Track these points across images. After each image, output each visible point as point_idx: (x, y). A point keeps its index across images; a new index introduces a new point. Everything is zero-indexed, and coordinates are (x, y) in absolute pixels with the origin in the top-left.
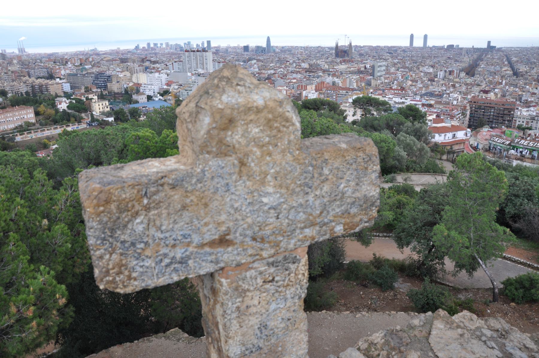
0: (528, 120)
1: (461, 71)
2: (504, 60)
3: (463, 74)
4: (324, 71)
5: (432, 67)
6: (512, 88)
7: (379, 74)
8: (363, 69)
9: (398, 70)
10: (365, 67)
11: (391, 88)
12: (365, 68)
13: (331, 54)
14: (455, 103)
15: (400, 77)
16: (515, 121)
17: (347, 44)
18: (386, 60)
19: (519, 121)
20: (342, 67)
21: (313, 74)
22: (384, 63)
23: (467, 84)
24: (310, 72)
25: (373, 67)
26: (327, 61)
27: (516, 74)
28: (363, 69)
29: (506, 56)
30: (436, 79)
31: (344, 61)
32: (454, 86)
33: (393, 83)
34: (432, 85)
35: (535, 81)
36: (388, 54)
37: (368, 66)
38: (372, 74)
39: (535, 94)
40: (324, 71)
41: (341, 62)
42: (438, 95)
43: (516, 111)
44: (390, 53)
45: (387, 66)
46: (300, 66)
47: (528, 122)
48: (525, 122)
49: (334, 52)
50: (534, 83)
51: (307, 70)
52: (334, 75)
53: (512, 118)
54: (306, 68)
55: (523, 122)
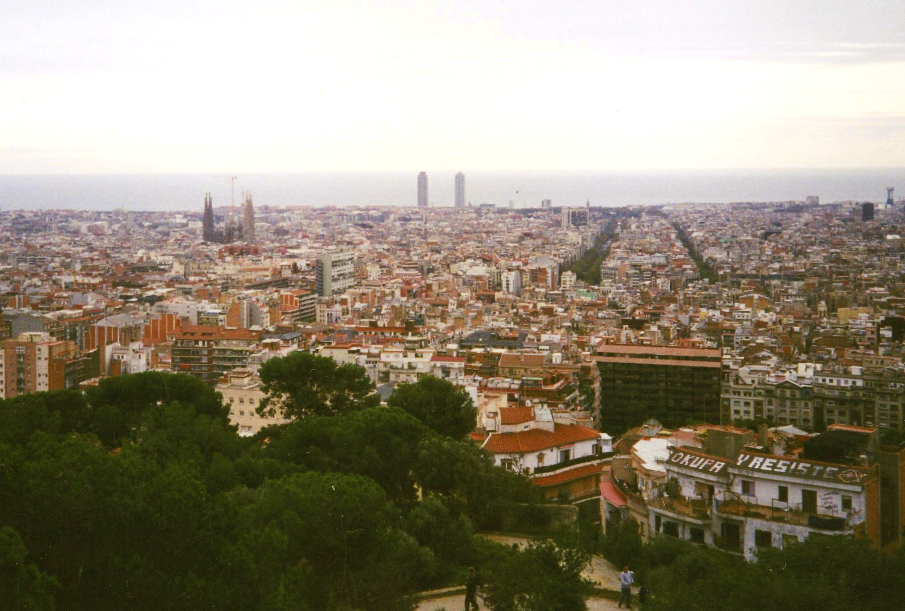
0: (760, 398)
1: (562, 269)
2: (673, 236)
3: (569, 278)
5: (485, 261)
6: (704, 310)
7: (336, 286)
8: (287, 273)
10: (295, 265)
11: (374, 325)
12: (295, 269)
14: (557, 357)
15: (398, 293)
17: (239, 202)
21: (138, 291)
23: (582, 307)
24: (128, 286)
27: (707, 270)
29: (675, 225)
30: (498, 295)
32: (549, 312)
34: (488, 311)
35: (757, 291)
37: (302, 264)
38: (318, 287)
39: (764, 324)
42: (507, 338)
44: (364, 226)
47: (758, 404)
48: (752, 404)
50: (756, 296)
52: (203, 294)
53: (718, 394)
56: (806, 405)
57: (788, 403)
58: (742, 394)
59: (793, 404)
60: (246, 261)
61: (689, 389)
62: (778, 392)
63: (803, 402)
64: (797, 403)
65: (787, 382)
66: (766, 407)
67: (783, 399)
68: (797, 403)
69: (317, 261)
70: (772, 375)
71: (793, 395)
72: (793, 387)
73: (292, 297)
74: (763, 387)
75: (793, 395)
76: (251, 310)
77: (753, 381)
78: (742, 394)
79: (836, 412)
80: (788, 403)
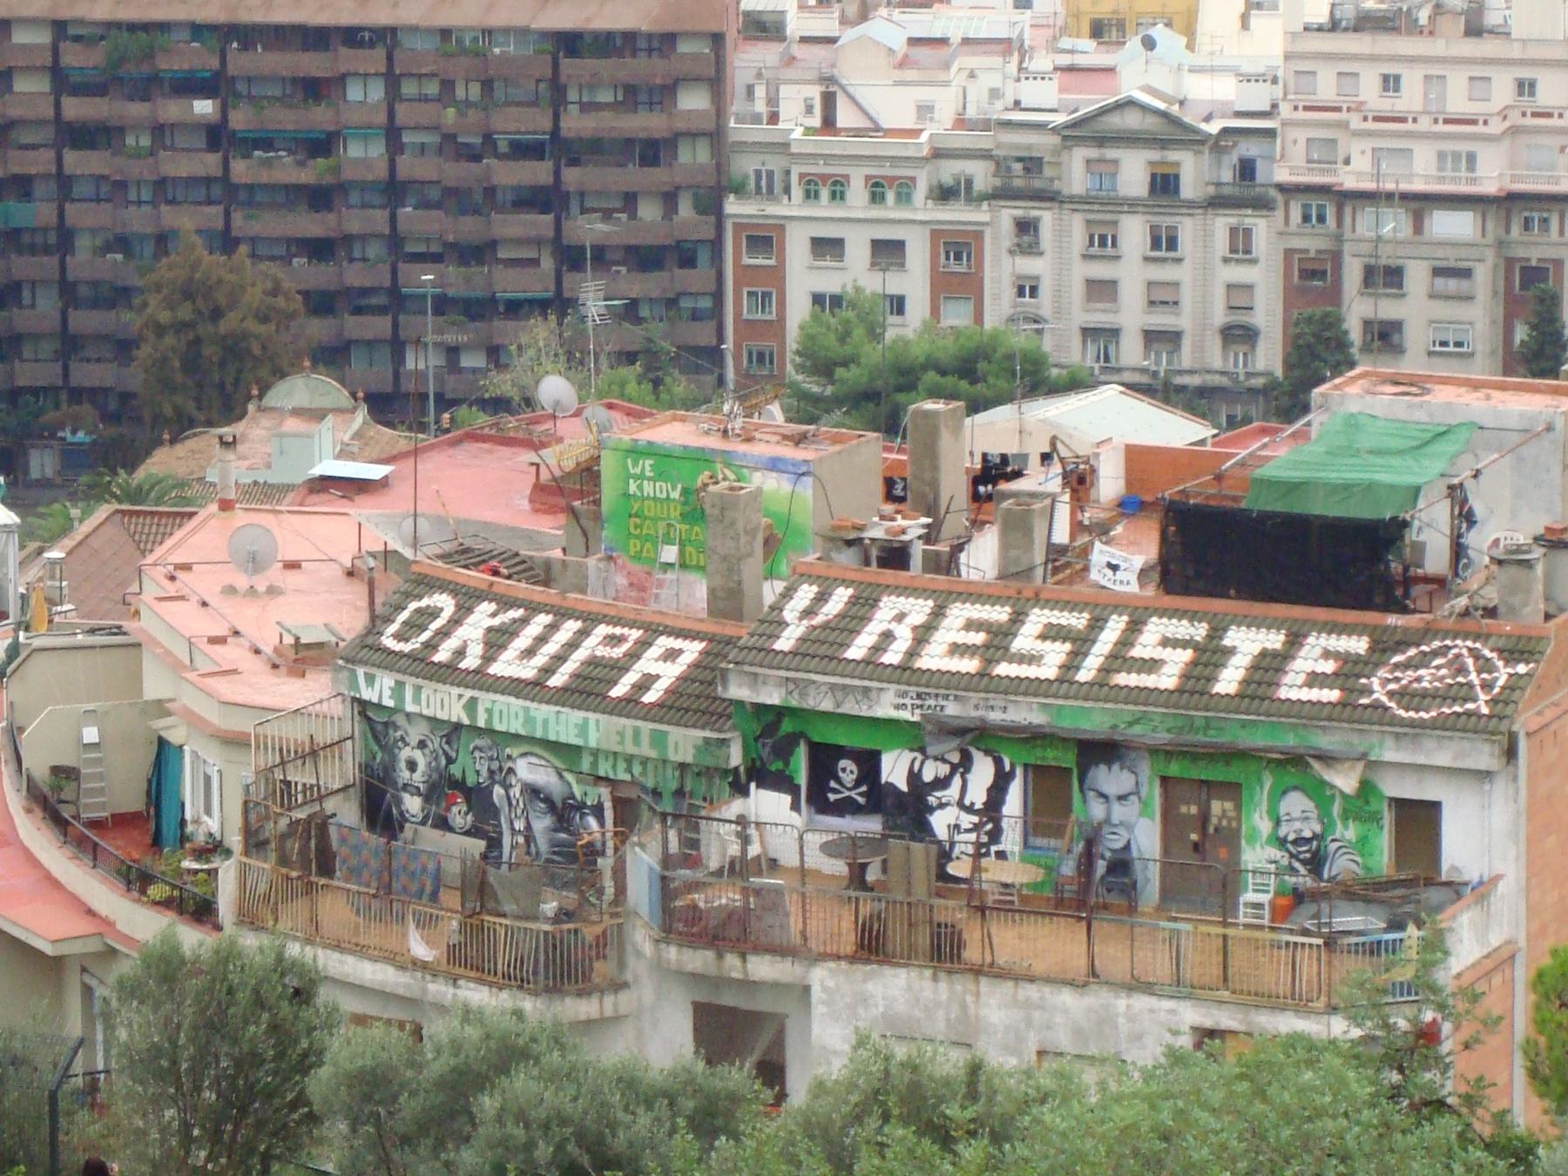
0: (957, 214)
16: (764, 239)
19: (828, 248)
43: (747, 60)
47: (958, 248)
53: (711, 205)
55: (888, 252)
56: (1241, 245)
57: (1134, 232)
58: (857, 192)
59: (1164, 242)
61: (538, 172)
62: (1075, 174)
63: (1221, 224)
64: (1188, 229)
65: (1130, 103)
66: (1000, 268)
67: (1102, 211)
68: (1188, 229)
70: (1042, 62)
71: (1164, 184)
72: (1172, 131)
74: (983, 140)
75: (1164, 184)
77: (925, 110)
78: (857, 192)
79: (1417, 276)
80: (1134, 232)
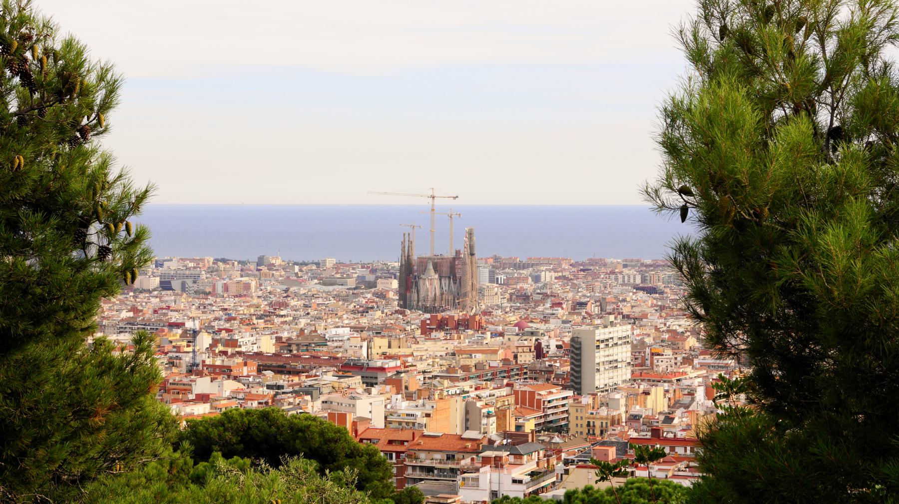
4: (348, 368)
7: (601, 380)
8: (527, 358)
9: (688, 361)
12: (539, 352)
13: (382, 295)
18: (633, 320)
20: (434, 350)
22: (623, 330)
25: (575, 350)
26: (364, 321)
28: (527, 358)
31: (442, 325)
33: (669, 419)
36: (641, 294)
37: (551, 344)
38: (574, 382)
40: (348, 368)
41: (426, 330)
44: (651, 291)
45: (638, 348)
46: (233, 343)
49: (395, 284)
51: (264, 363)
54: (259, 355)
60: (465, 340)
69: (573, 340)
73: (532, 394)
76: (467, 412)
